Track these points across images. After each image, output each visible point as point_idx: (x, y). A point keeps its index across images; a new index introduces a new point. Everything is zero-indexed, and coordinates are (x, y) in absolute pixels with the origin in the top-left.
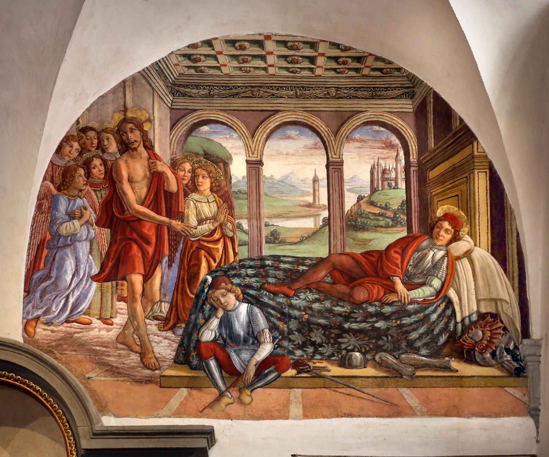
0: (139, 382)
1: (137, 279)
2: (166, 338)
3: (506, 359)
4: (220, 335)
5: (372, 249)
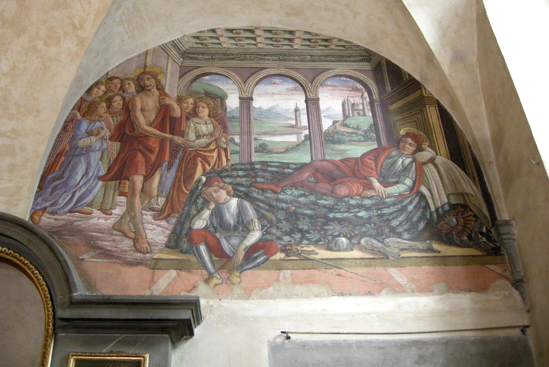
1: (139, 180)
2: (159, 226)
3: (481, 240)
4: (212, 223)
5: (348, 156)
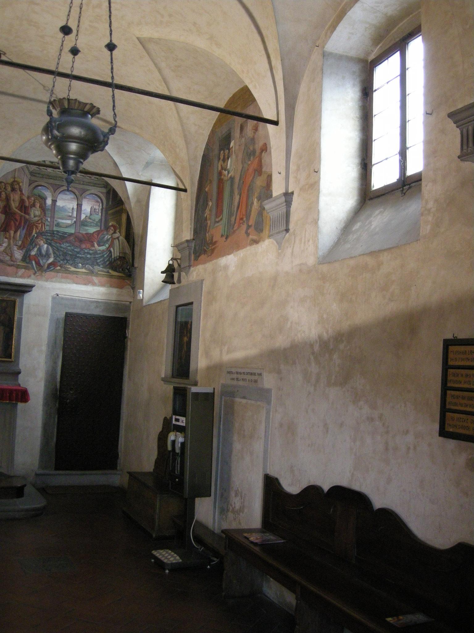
0: (9, 265)
1: (12, 232)
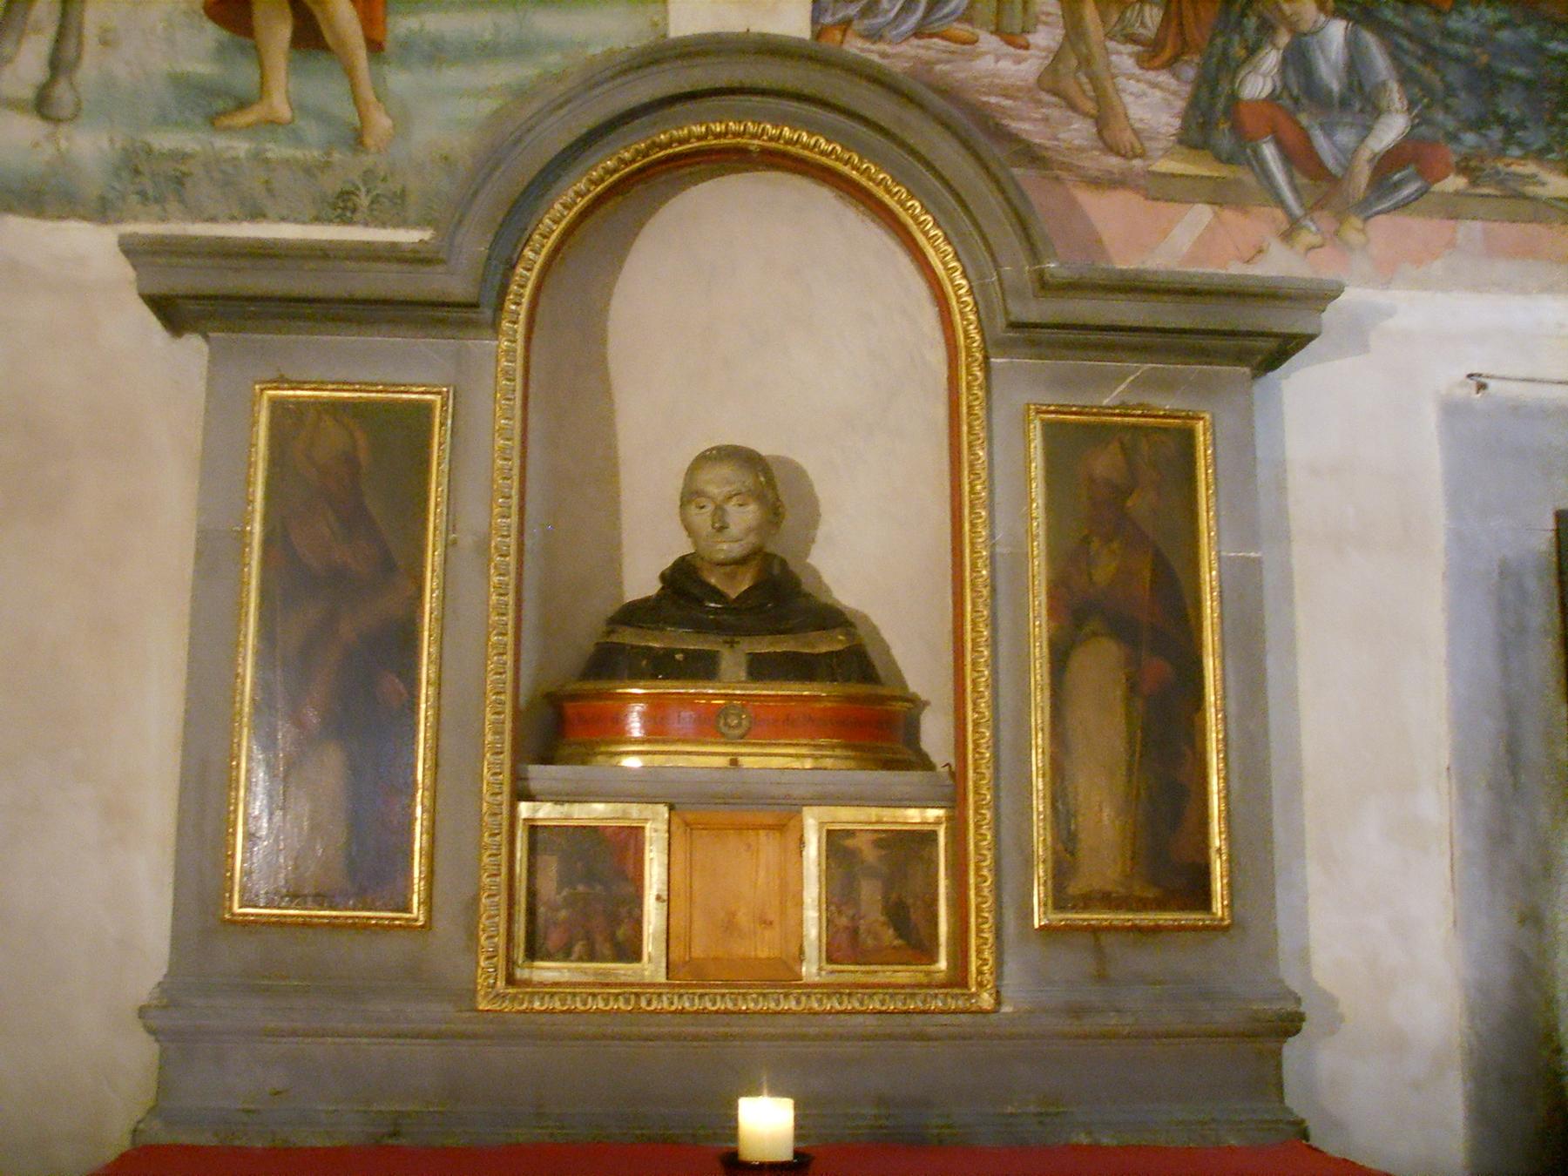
2: (1154, 85)
4: (1285, 86)
